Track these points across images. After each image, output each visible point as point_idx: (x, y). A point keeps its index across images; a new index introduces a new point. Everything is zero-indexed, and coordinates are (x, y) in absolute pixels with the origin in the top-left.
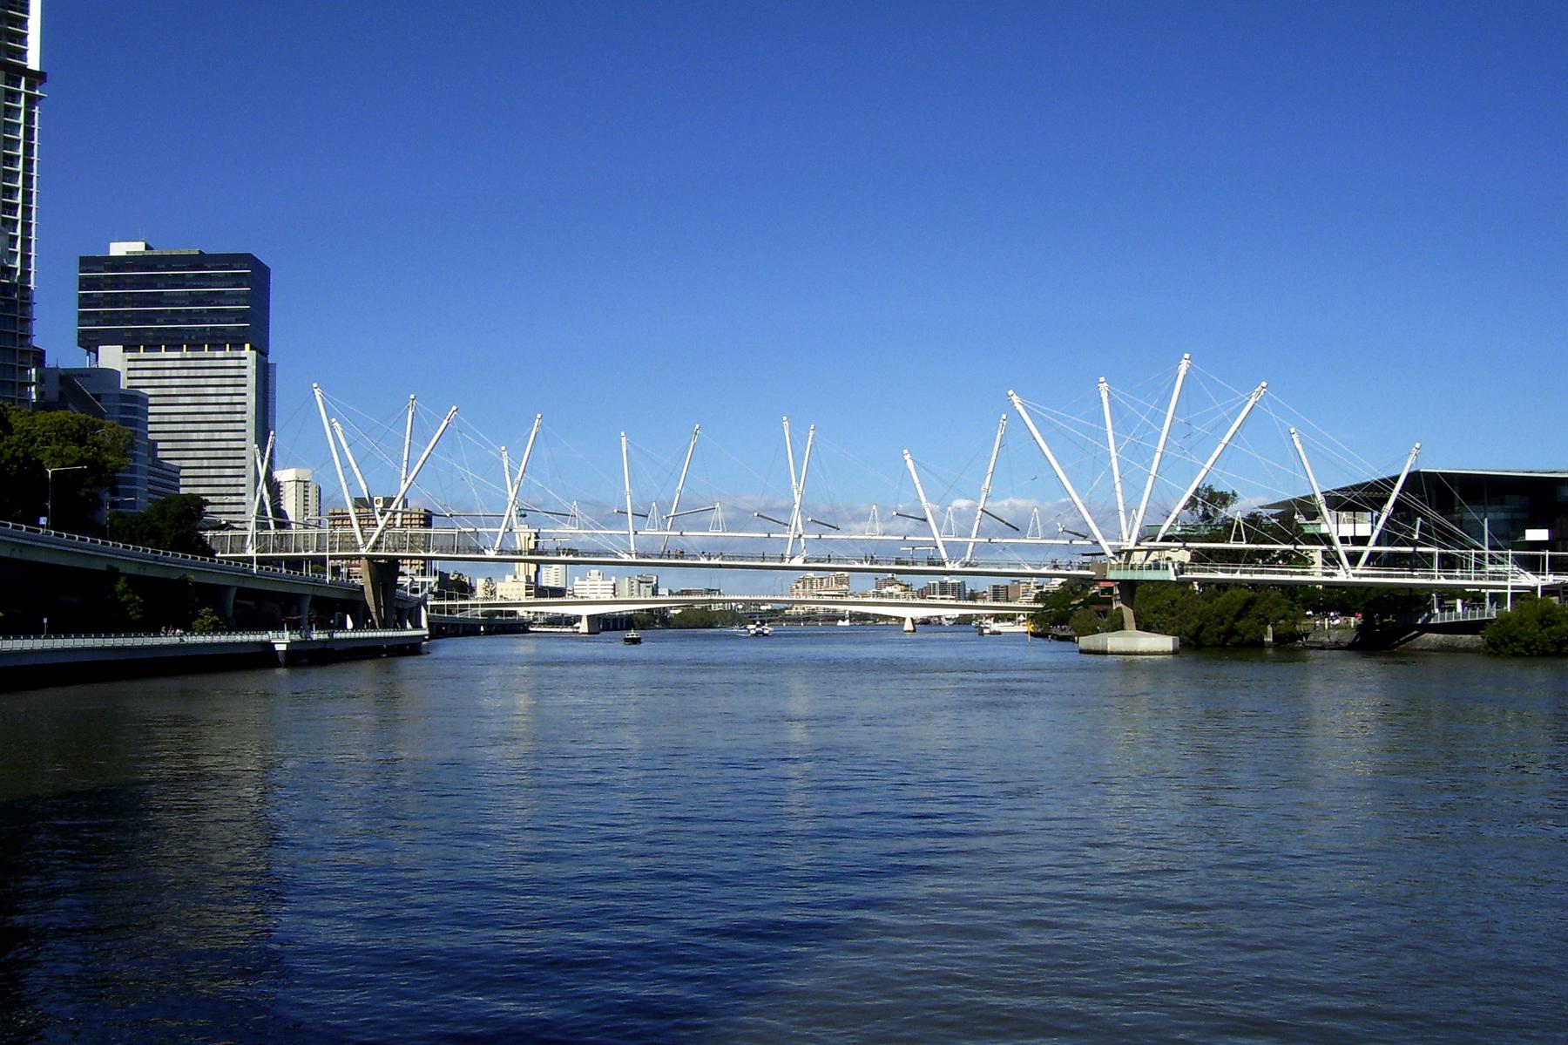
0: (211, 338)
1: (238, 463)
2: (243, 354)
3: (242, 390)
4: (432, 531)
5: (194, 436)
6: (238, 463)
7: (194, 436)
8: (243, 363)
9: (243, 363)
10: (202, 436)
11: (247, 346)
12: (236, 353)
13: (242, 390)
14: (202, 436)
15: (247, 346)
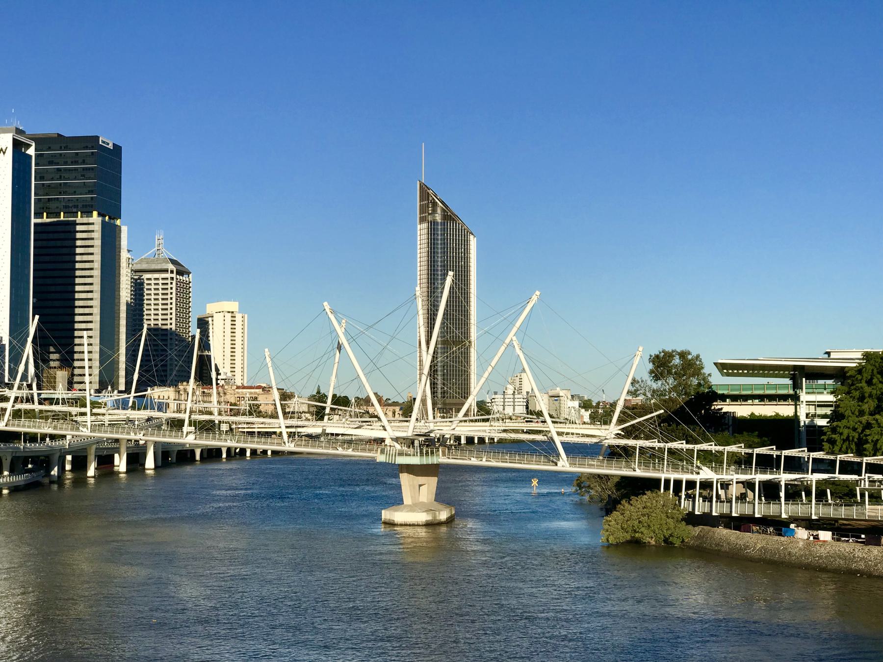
0: (66, 207)
1: (87, 311)
2: (91, 220)
3: (90, 250)
4: (274, 384)
5: (53, 289)
6: (87, 311)
7: (53, 289)
8: (91, 228)
9: (91, 228)
10: (59, 288)
11: (95, 213)
12: (85, 220)
13: (90, 250)
14: (59, 288)
15: (95, 213)
